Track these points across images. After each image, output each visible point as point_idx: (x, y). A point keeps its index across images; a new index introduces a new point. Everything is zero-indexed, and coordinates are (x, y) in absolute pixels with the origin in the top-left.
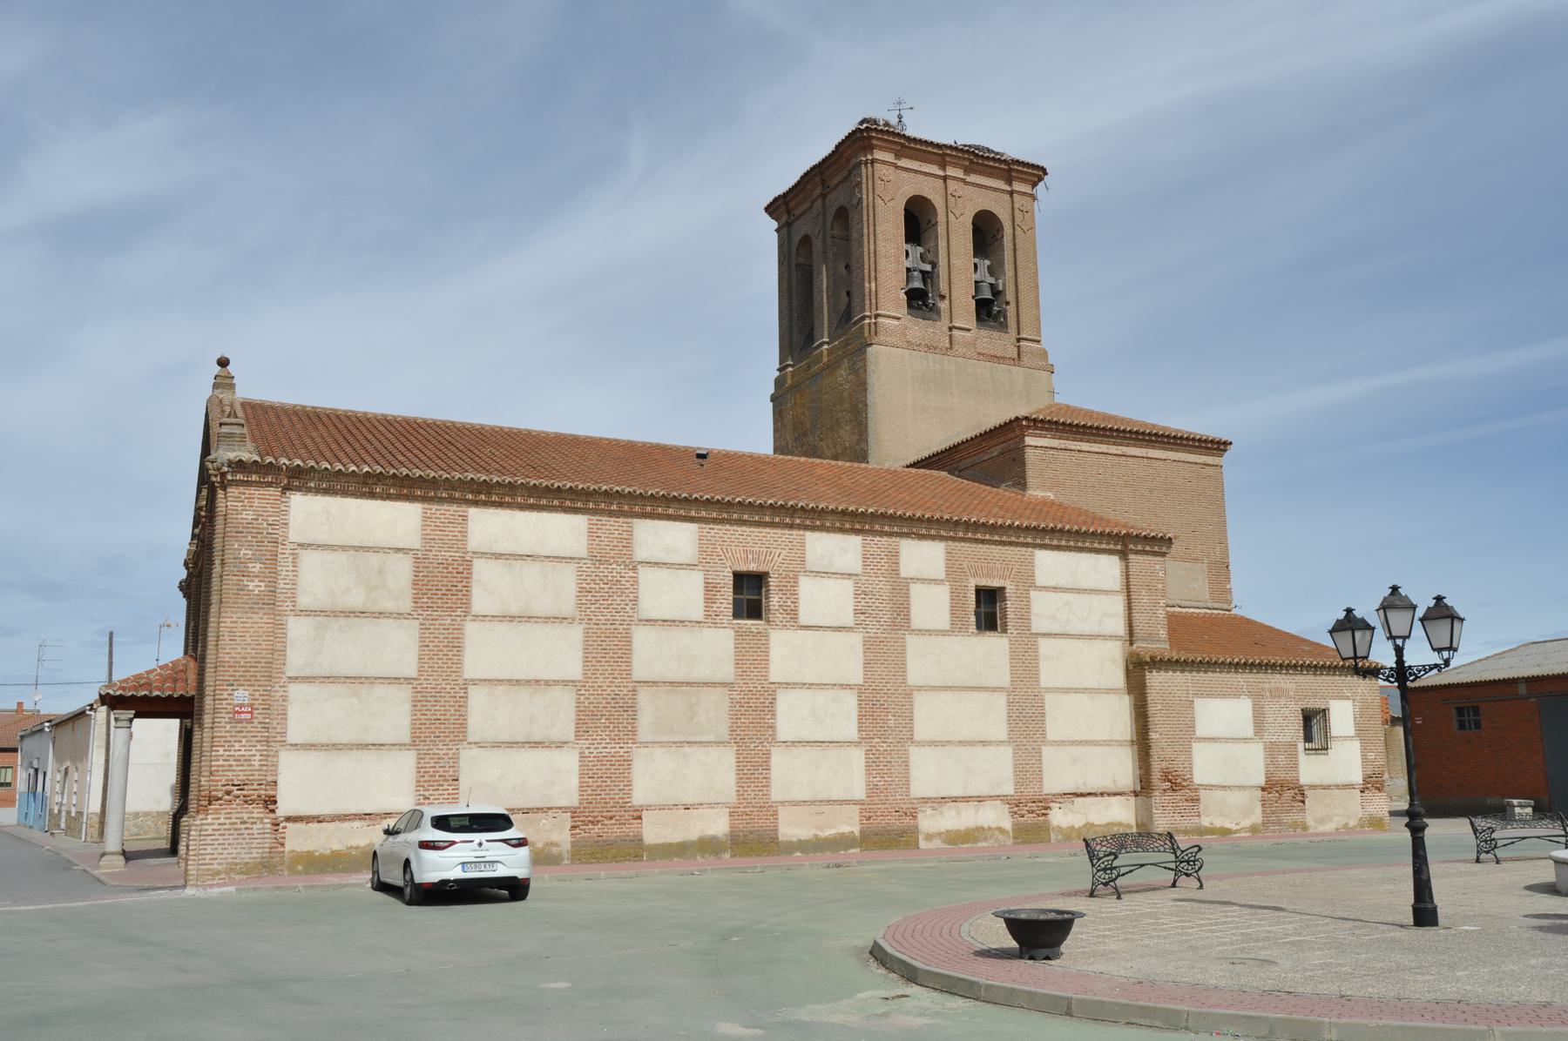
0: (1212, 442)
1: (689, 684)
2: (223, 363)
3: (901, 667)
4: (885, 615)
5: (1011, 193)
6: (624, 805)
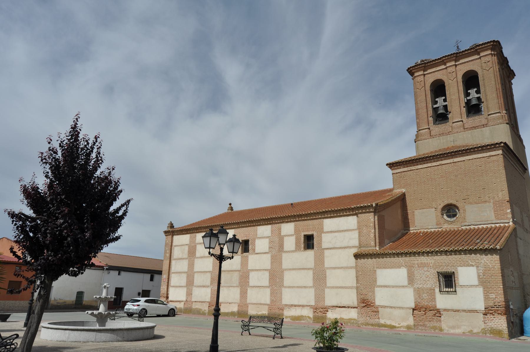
0: (488, 145)
1: (232, 271)
2: (230, 204)
4: (277, 248)
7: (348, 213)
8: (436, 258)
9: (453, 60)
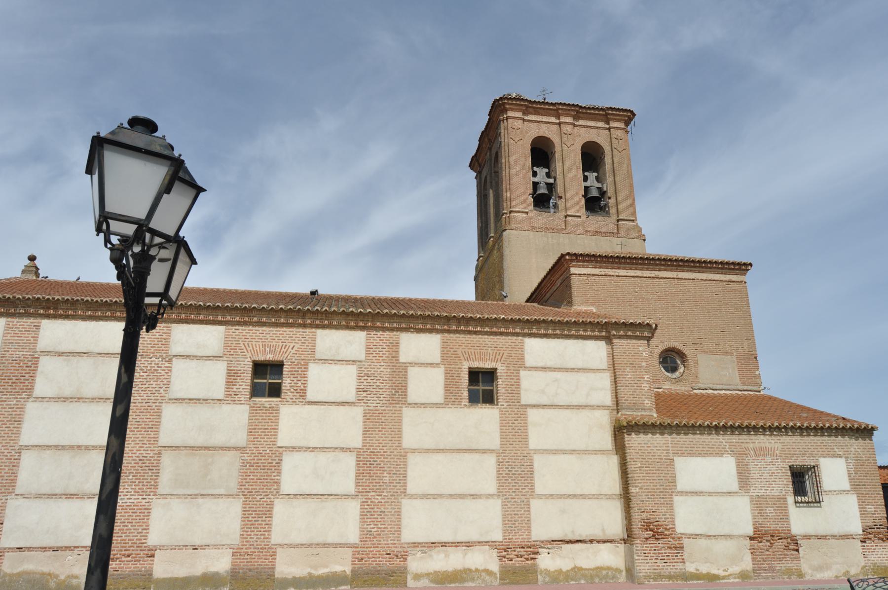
1: (207, 448)
2: (32, 258)
3: (397, 433)
4: (385, 394)
5: (609, 129)
6: (141, 546)
7: (589, 333)
8: (784, 439)
9: (571, 116)
